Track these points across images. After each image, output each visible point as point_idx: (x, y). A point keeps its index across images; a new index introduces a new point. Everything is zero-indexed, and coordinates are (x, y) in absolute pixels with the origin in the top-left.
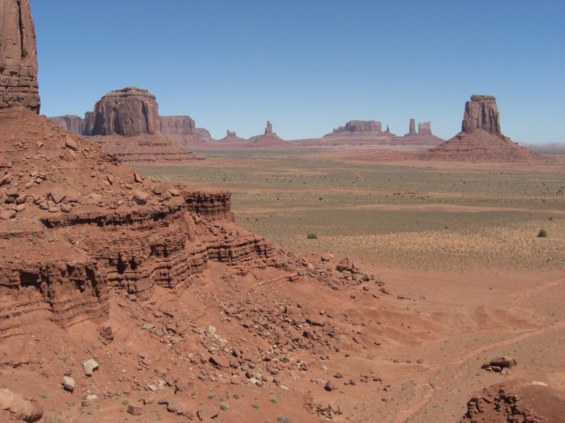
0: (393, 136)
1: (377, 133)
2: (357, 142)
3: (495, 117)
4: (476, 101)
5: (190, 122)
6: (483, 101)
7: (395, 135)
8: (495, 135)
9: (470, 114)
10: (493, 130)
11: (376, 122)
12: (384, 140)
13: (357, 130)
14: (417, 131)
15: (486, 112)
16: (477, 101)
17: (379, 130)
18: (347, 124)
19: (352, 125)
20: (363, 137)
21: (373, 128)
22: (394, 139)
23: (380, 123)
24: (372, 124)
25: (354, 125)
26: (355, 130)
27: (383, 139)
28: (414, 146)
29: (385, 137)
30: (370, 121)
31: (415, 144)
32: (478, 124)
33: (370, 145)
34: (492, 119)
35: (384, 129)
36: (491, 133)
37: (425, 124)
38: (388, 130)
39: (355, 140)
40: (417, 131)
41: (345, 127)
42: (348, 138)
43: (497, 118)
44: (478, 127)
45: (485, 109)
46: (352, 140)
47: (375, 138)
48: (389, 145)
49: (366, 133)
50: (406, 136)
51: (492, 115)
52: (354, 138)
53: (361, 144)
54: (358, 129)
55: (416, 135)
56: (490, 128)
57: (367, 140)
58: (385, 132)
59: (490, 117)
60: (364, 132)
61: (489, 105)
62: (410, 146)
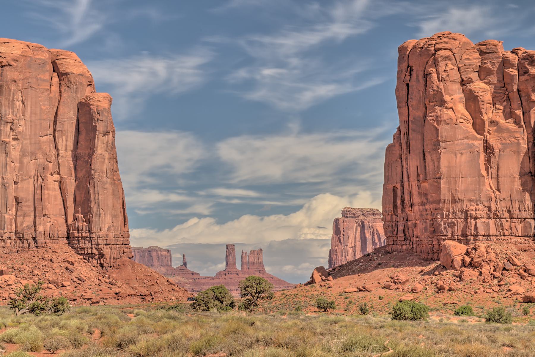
0: (195, 276)
6: (362, 217)
7: (198, 274)
9: (342, 238)
11: (160, 249)
14: (239, 267)
15: (368, 235)
17: (167, 265)
21: (156, 262)
22: (197, 280)
23: (168, 251)
24: (154, 254)
29: (180, 278)
30: (150, 247)
38: (185, 264)
40: (239, 267)
45: (366, 231)
55: (238, 274)
58: (179, 269)
61: (371, 225)
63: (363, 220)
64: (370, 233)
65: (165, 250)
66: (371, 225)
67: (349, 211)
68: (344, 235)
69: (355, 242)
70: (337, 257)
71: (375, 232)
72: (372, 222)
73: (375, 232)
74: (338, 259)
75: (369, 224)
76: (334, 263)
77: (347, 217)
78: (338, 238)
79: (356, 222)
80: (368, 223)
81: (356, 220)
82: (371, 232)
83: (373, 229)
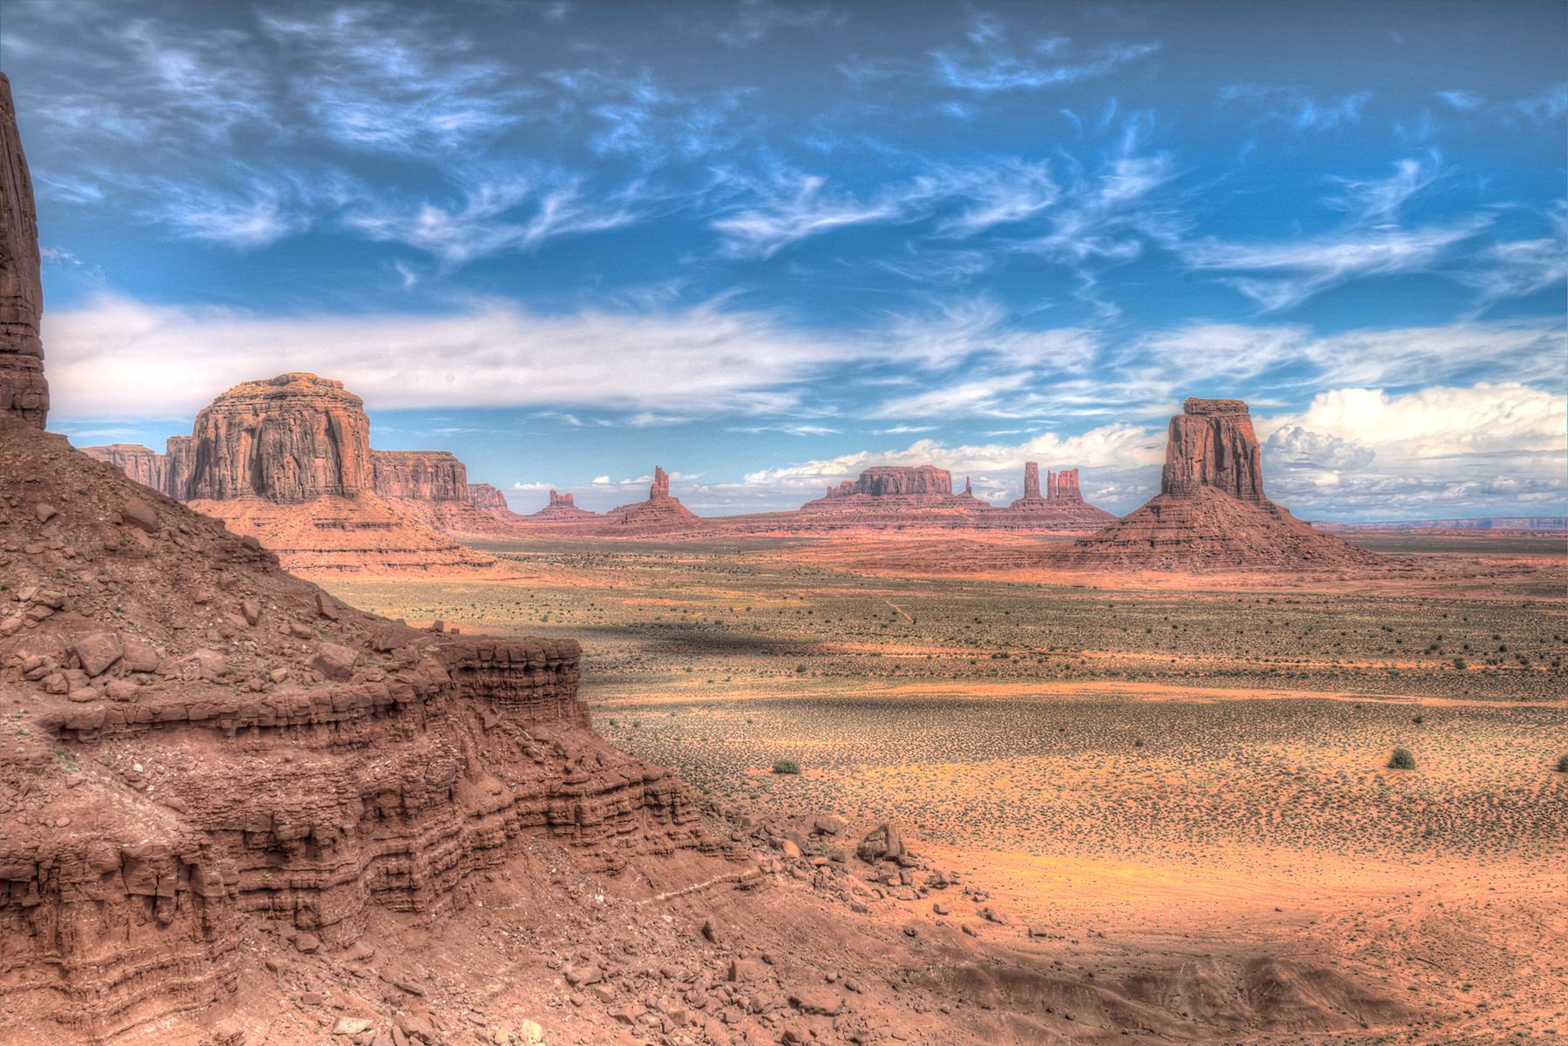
0: (983, 507)
1: (940, 498)
2: (889, 523)
3: (1250, 456)
5: (318, 599)
9: (1183, 447)
11: (937, 471)
12: (961, 517)
13: (888, 490)
14: (1044, 493)
15: (1226, 442)
16: (1201, 414)
18: (863, 477)
19: (876, 478)
20: (904, 510)
21: (930, 488)
24: (927, 476)
25: (880, 479)
26: (883, 490)
27: (957, 514)
28: (1037, 532)
29: (961, 509)
31: (1040, 526)
32: (1204, 474)
33: (922, 530)
34: (1242, 460)
35: (957, 490)
37: (1064, 474)
38: (969, 490)
39: (883, 517)
40: (1044, 493)
41: (857, 483)
42: (865, 510)
44: (1205, 481)
45: (1223, 436)
46: (876, 517)
47: (936, 511)
48: (973, 530)
49: (912, 499)
50: (1015, 505)
51: (1240, 450)
52: (881, 512)
53: (900, 528)
54: (891, 488)
55: (1042, 504)
56: (1235, 483)
57: (915, 518)
58: (962, 496)
59: (1236, 455)
60: (907, 496)
62: (1027, 532)
65: (943, 471)
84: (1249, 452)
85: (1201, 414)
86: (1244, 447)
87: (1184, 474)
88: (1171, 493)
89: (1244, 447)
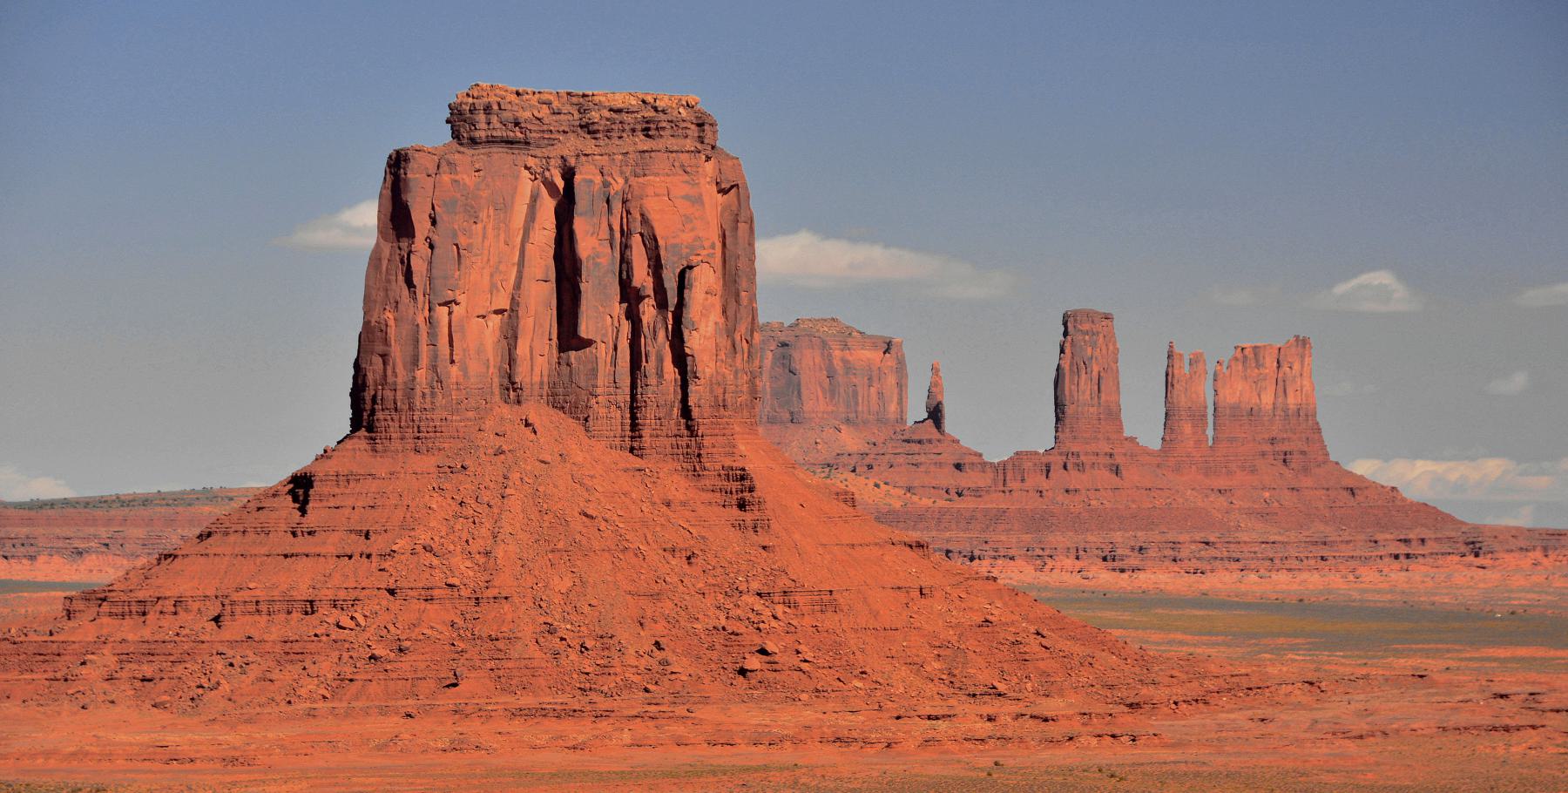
3: (672, 300)
4: (491, 141)
6: (570, 146)
8: (671, 465)
9: (418, 265)
10: (648, 417)
15: (591, 242)
16: (509, 142)
32: (512, 361)
34: (648, 311)
36: (632, 450)
43: (681, 304)
44: (511, 387)
45: (580, 225)
51: (642, 277)
56: (624, 396)
59: (630, 296)
61: (618, 184)
63: (572, 162)
64: (605, 234)
66: (618, 184)
67: (487, 109)
68: (432, 247)
69: (518, 285)
70: (389, 372)
71: (637, 226)
72: (628, 171)
73: (637, 226)
74: (390, 379)
75: (606, 185)
76: (374, 398)
77: (474, 142)
78: (402, 262)
79: (526, 168)
80: (598, 179)
81: (531, 162)
82: (617, 228)
83: (628, 212)
84: (671, 284)
85: (509, 142)
86: (656, 266)
87: (415, 361)
88: (370, 429)
89: (656, 266)
